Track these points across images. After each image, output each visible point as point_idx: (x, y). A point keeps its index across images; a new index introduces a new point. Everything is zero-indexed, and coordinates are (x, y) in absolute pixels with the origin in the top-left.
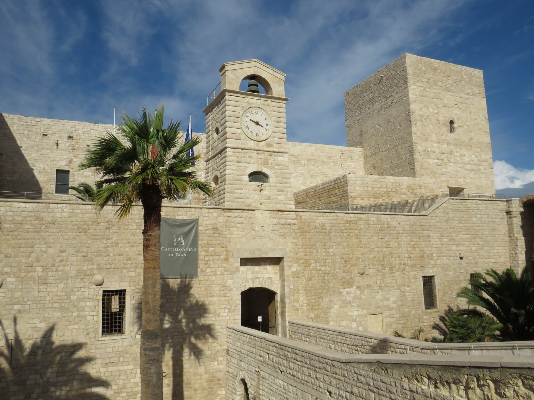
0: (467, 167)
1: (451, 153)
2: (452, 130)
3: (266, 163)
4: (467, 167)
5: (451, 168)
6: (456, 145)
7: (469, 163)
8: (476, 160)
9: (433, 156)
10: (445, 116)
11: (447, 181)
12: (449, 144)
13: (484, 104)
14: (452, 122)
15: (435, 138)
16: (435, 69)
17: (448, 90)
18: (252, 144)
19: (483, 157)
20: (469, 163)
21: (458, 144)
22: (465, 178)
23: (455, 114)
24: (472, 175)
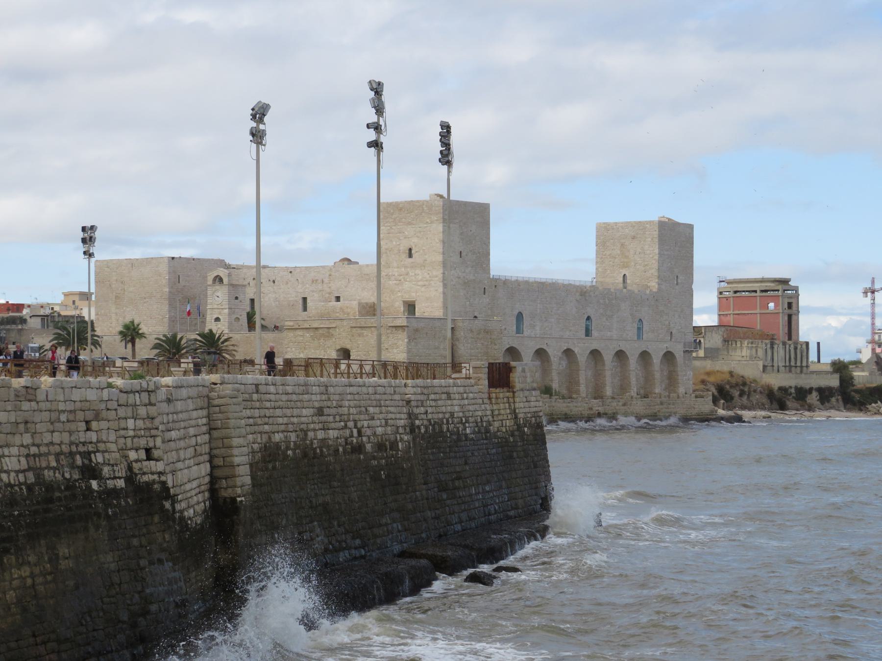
0: (420, 283)
1: (407, 274)
2: (410, 256)
3: (220, 313)
4: (420, 283)
5: (406, 285)
6: (412, 267)
7: (421, 280)
8: (428, 277)
9: (393, 278)
10: (404, 245)
11: (402, 296)
12: (406, 267)
13: (440, 228)
14: (410, 250)
15: (395, 264)
16: (401, 209)
17: (409, 224)
18: (216, 306)
19: (435, 273)
20: (421, 280)
21: (413, 267)
22: (416, 292)
23: (414, 242)
24: (423, 289)
